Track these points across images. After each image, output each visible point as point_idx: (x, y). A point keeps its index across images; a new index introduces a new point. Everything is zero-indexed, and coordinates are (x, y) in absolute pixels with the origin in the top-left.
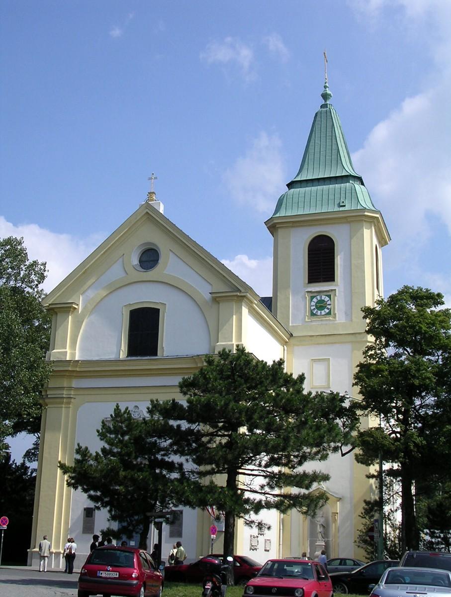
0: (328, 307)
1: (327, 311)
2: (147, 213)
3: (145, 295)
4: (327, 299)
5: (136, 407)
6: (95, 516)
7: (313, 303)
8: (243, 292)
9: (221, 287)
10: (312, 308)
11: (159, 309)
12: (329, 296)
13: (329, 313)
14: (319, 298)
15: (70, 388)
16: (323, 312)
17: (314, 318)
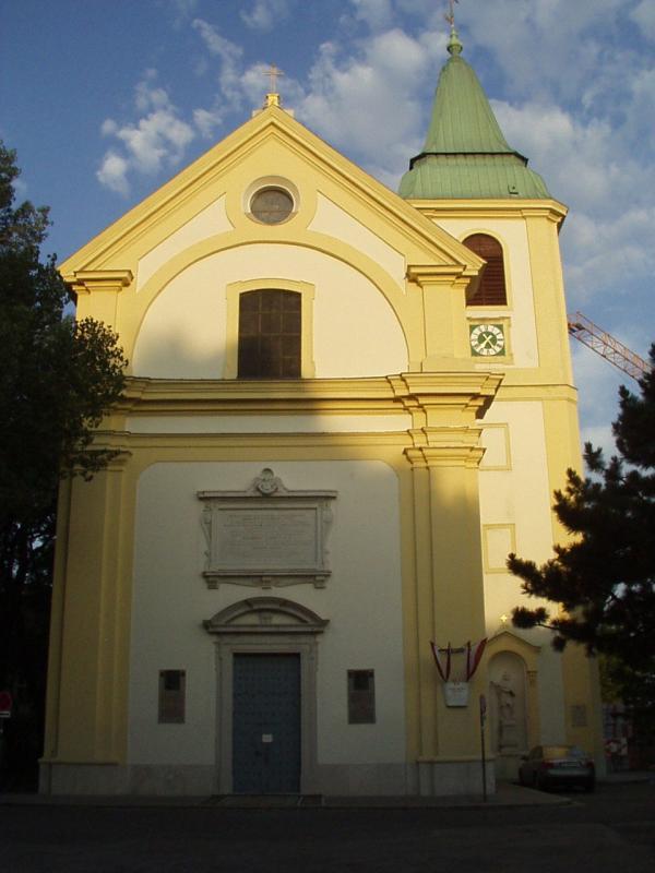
0: (501, 343)
1: (498, 349)
2: (272, 124)
3: (271, 266)
4: (496, 331)
5: (268, 470)
6: (184, 685)
7: (474, 337)
8: (470, 270)
9: (423, 258)
10: (473, 343)
11: (298, 295)
12: (500, 327)
13: (502, 353)
14: (483, 328)
16: (492, 352)
17: (479, 358)
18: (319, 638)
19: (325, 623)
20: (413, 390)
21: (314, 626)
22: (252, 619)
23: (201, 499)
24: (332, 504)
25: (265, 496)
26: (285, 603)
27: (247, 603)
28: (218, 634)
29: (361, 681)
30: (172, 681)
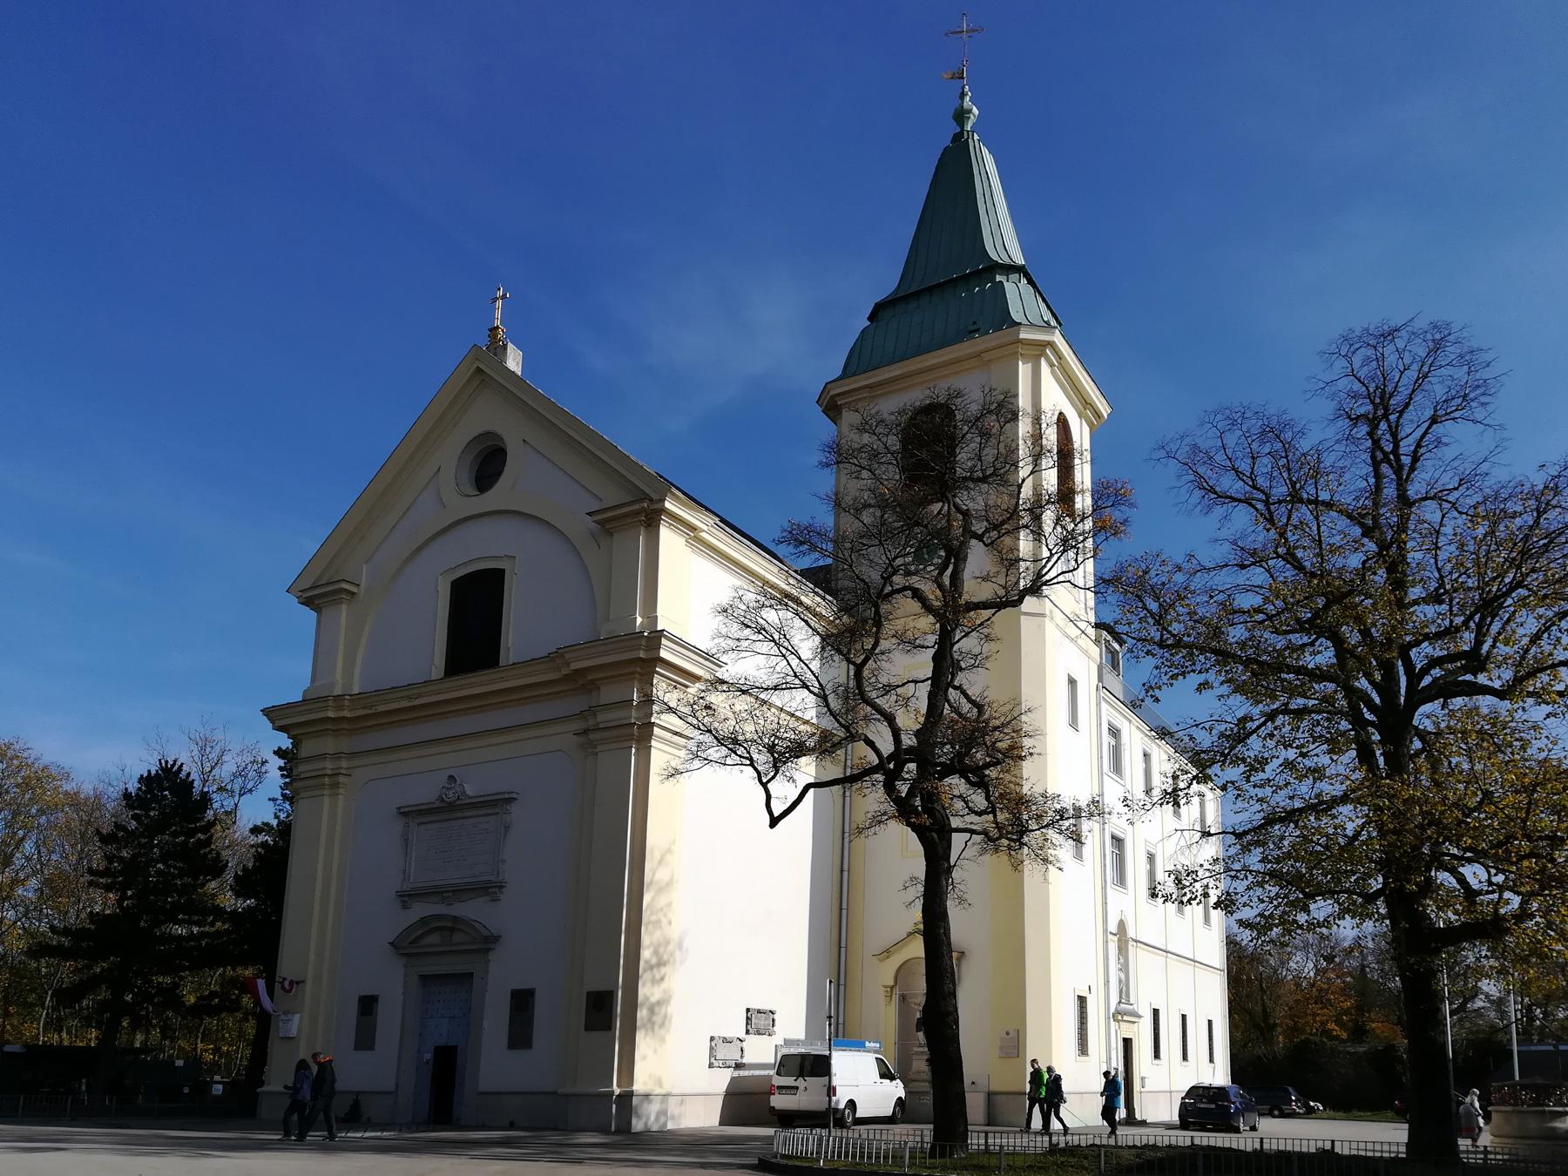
5: (451, 777)
11: (499, 574)
15: (337, 756)
18: (491, 956)
19: (497, 939)
20: (574, 666)
21: (487, 942)
22: (434, 939)
23: (404, 814)
24: (514, 808)
25: (448, 808)
26: (455, 919)
27: (423, 921)
28: (408, 955)
29: (522, 1001)
30: (368, 1005)
